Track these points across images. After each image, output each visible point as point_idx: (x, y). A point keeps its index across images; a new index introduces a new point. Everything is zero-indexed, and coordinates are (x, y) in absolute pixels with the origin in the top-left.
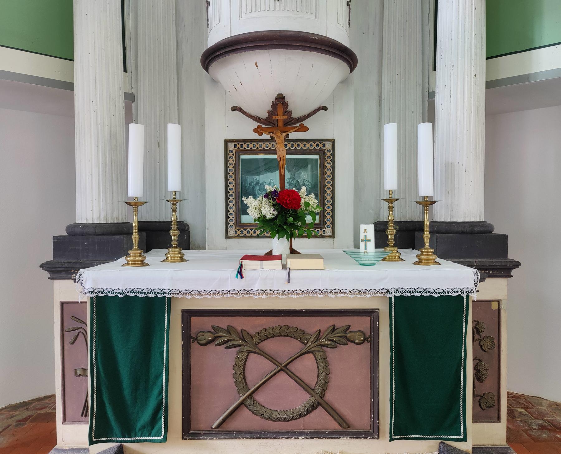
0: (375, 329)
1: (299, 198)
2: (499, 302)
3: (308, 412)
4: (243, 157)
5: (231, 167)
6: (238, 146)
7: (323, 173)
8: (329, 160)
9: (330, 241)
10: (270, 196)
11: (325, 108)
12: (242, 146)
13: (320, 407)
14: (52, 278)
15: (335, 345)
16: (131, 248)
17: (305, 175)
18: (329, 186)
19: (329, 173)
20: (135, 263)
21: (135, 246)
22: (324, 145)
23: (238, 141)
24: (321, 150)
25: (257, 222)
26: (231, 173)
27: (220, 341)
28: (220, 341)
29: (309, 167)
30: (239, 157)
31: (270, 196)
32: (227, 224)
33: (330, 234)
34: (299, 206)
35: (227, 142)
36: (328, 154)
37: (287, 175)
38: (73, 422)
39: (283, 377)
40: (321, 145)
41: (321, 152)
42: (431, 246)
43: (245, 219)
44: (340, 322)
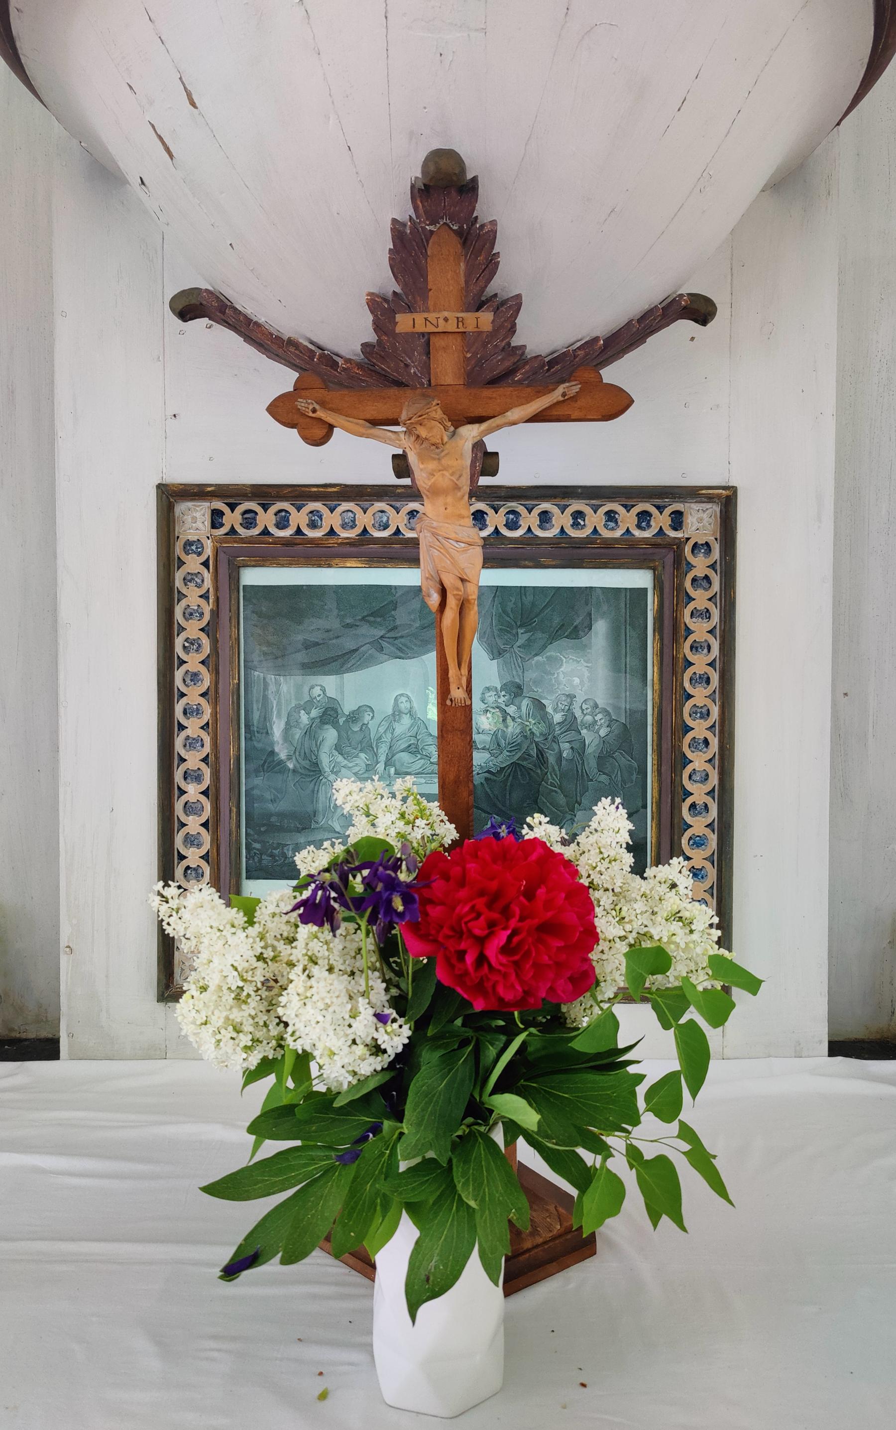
4: (252, 577)
5: (193, 629)
6: (233, 519)
8: (700, 598)
12: (249, 520)
18: (700, 729)
19: (700, 663)
22: (677, 520)
24: (660, 542)
26: (193, 662)
29: (601, 628)
30: (235, 579)
36: (700, 565)
40: (661, 520)
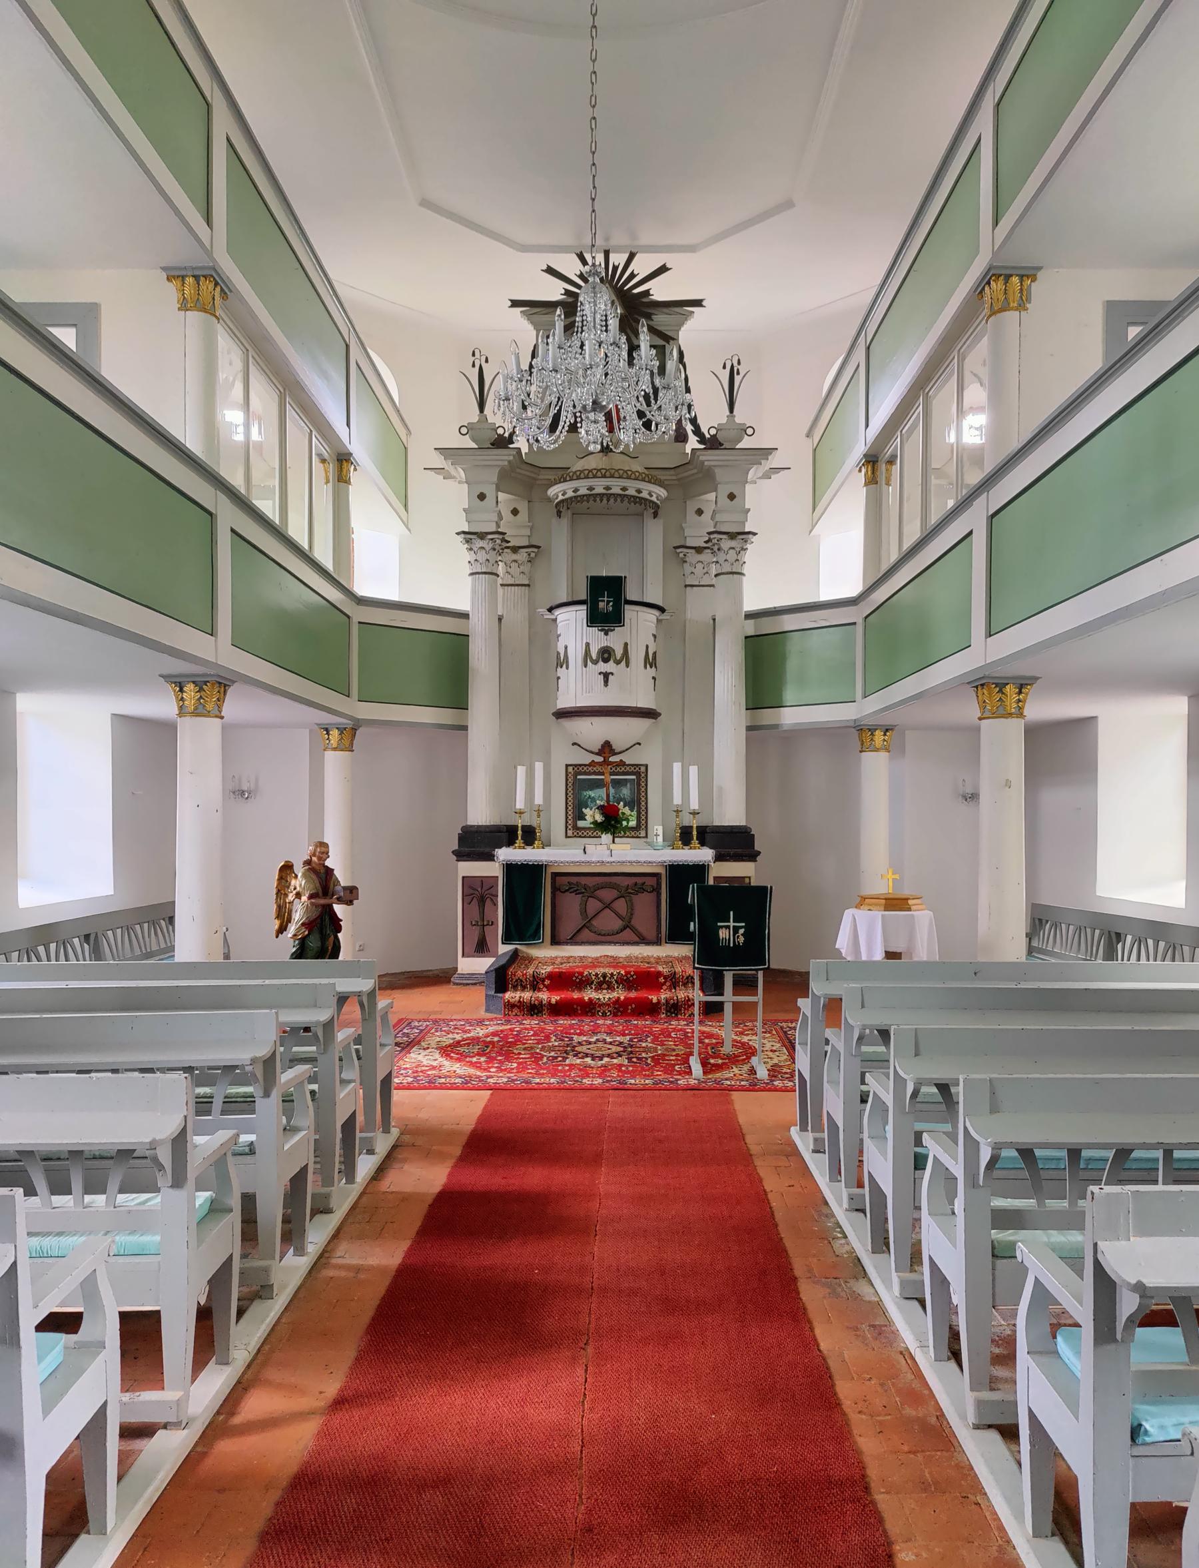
0: (659, 884)
1: (619, 810)
2: (750, 878)
3: (621, 931)
4: (579, 777)
5: (570, 785)
6: (576, 769)
7: (639, 790)
8: (643, 780)
9: (645, 840)
10: (601, 808)
11: (639, 744)
13: (628, 929)
14: (458, 860)
15: (637, 892)
16: (517, 839)
17: (626, 792)
18: (643, 799)
20: (520, 847)
21: (520, 838)
23: (576, 765)
25: (592, 826)
26: (570, 789)
27: (572, 890)
28: (572, 890)
29: (628, 785)
31: (601, 808)
32: (566, 827)
33: (644, 835)
34: (618, 815)
35: (567, 766)
36: (643, 775)
37: (612, 791)
38: (469, 956)
39: (607, 910)
40: (637, 769)
41: (638, 774)
42: (697, 839)
43: (581, 824)
44: (639, 880)
